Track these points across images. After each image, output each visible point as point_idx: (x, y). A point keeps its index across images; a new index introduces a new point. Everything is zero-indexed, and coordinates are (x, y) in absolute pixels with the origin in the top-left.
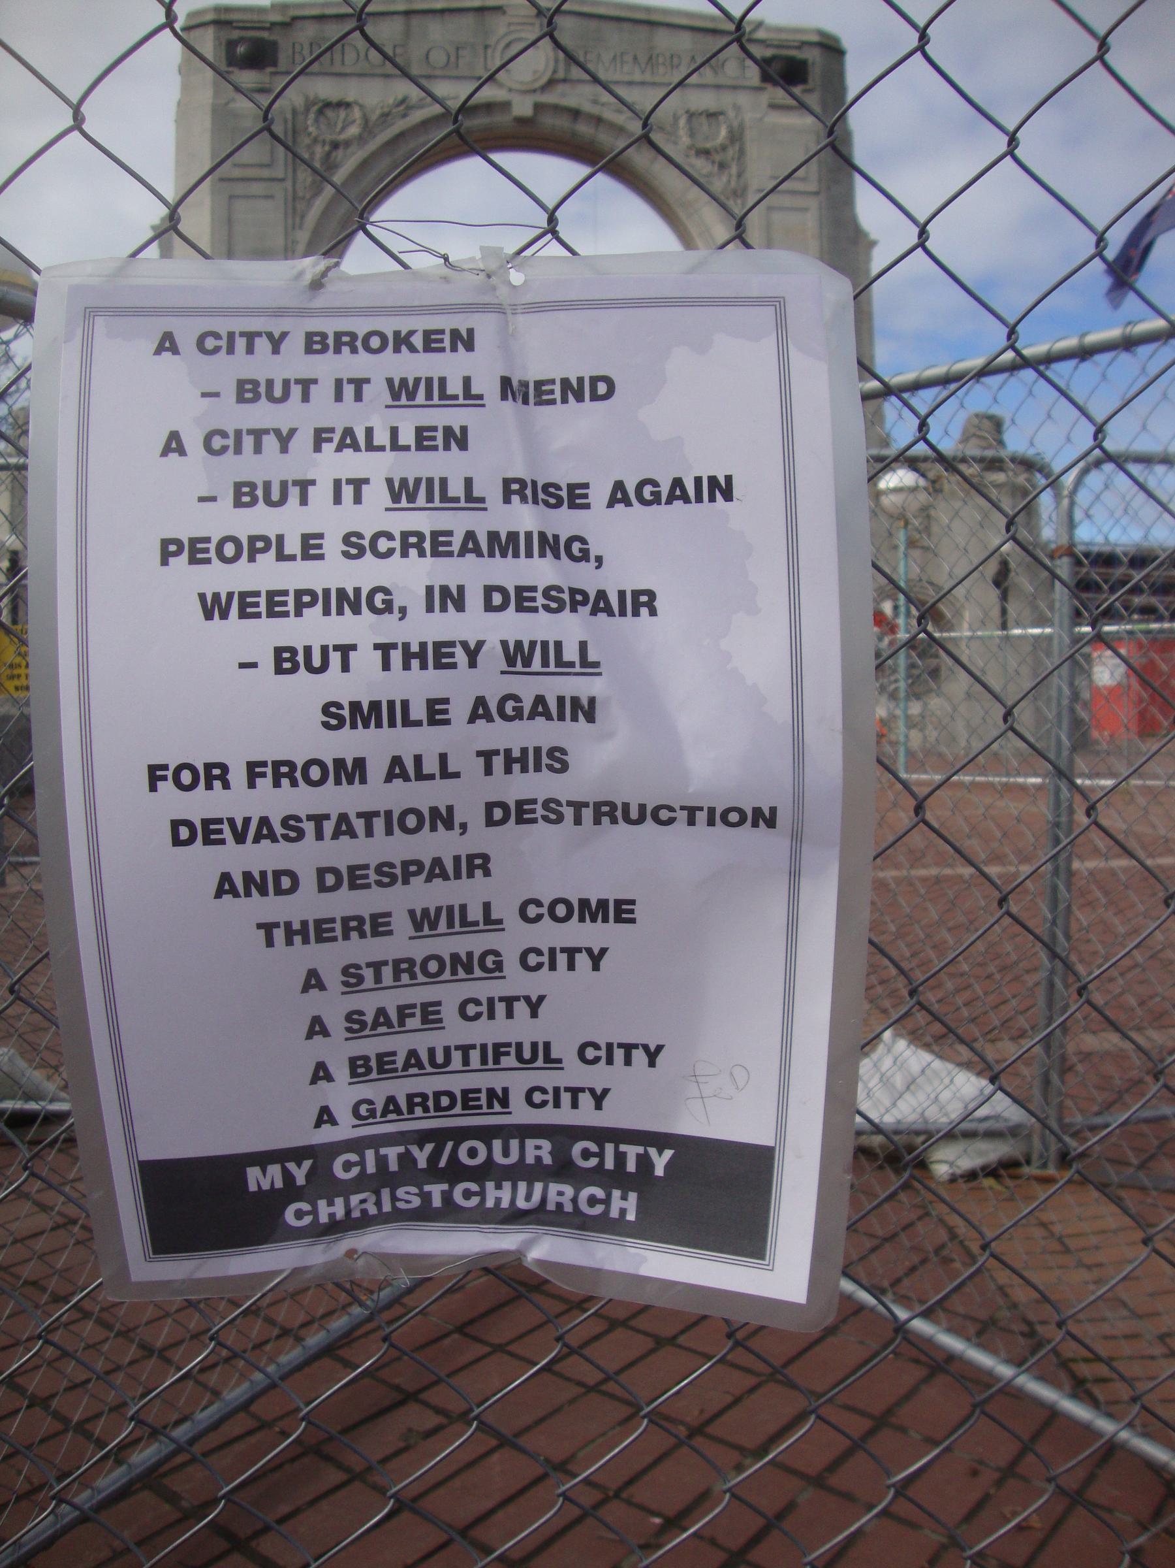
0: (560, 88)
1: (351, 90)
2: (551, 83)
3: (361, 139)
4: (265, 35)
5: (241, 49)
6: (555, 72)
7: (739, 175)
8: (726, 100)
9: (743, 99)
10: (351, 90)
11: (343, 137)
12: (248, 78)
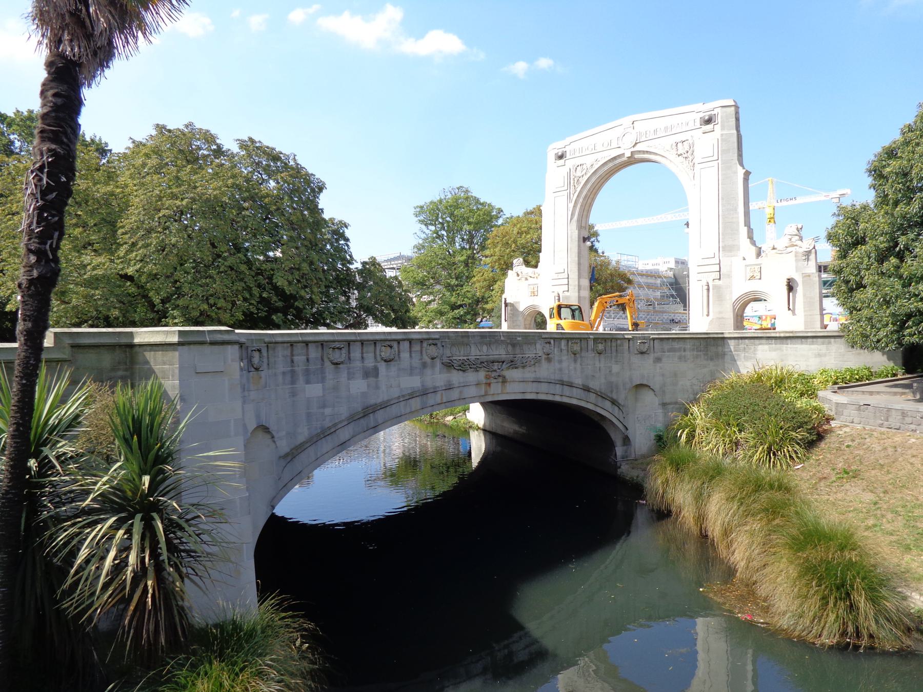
0: (638, 145)
2: (636, 143)
12: (561, 162)
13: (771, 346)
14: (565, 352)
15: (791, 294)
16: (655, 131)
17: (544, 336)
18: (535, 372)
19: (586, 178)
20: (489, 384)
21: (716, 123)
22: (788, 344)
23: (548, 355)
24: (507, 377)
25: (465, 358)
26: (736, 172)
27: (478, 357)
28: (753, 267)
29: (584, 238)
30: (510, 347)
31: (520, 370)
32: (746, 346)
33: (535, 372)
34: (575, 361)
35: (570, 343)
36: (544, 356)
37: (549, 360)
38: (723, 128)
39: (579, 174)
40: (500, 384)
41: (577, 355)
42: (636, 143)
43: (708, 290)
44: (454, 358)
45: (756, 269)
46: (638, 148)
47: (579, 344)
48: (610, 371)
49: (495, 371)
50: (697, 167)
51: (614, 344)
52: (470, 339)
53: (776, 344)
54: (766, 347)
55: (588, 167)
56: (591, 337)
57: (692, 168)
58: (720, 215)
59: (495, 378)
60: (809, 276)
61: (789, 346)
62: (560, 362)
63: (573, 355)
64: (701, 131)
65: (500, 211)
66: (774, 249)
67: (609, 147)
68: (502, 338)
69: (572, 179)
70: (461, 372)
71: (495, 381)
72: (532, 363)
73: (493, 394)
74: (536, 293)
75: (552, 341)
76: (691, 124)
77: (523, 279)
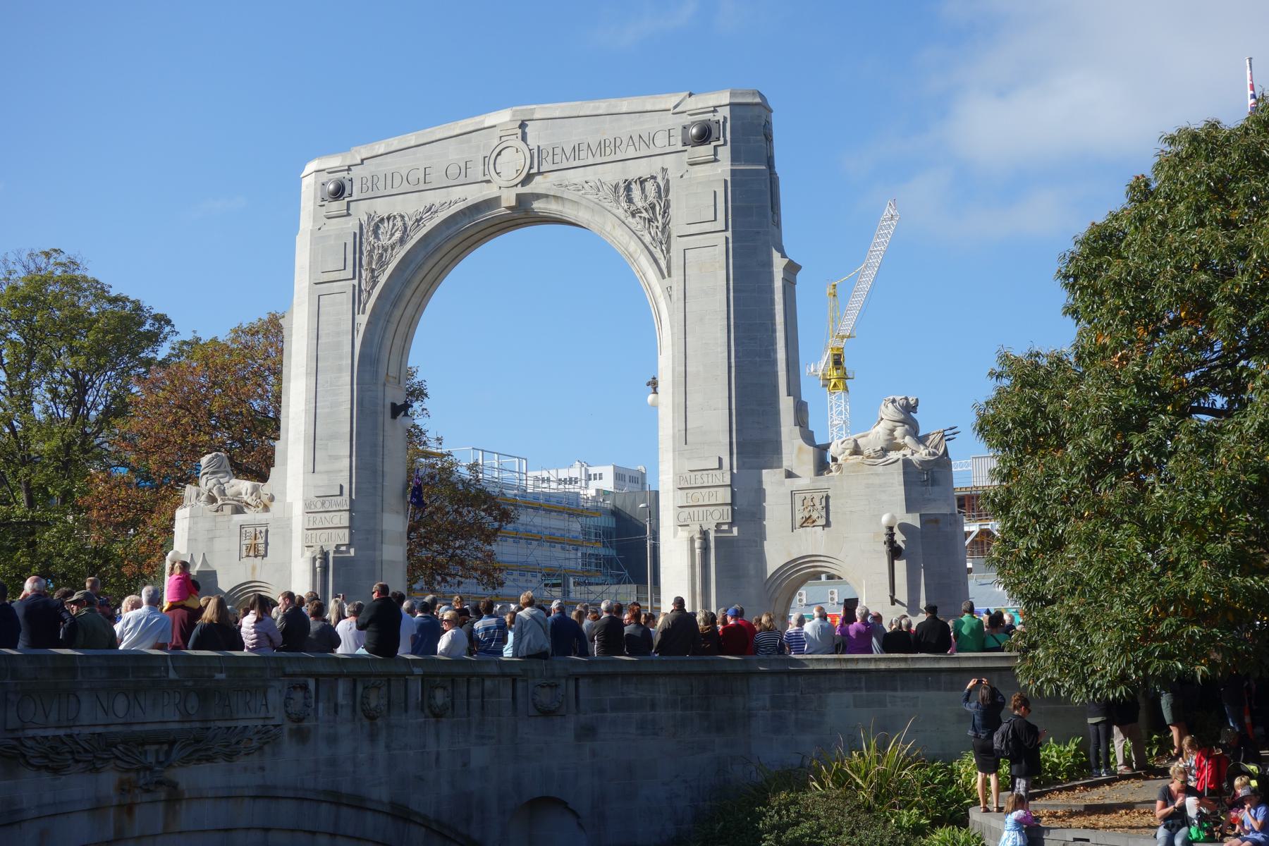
3: (402, 241)
6: (531, 168)
8: (658, 163)
9: (669, 161)
11: (390, 242)
12: (337, 206)
13: (857, 693)
14: (345, 713)
16: (576, 150)
17: (289, 670)
18: (262, 769)
19: (401, 253)
20: (130, 808)
22: (895, 689)
23: (300, 720)
24: (183, 785)
25: (61, 732)
26: (769, 264)
27: (99, 730)
29: (393, 405)
30: (193, 703)
31: (221, 764)
32: (798, 694)
33: (262, 769)
34: (373, 737)
35: (360, 689)
36: (288, 726)
37: (301, 736)
38: (735, 158)
39: (385, 240)
40: (161, 807)
41: (379, 722)
43: (705, 549)
44: (30, 733)
45: (817, 501)
46: (538, 185)
47: (384, 689)
48: (465, 765)
49: (149, 768)
50: (677, 245)
51: (475, 691)
52: (80, 678)
53: (869, 689)
54: (847, 697)
56: (417, 671)
58: (733, 364)
59: (148, 791)
60: (936, 521)
61: (899, 694)
62: (333, 740)
63: (366, 722)
64: (685, 157)
65: (163, 320)
67: (462, 179)
68: (172, 675)
70: (46, 777)
71: (146, 797)
72: (255, 744)
73: (140, 837)
74: (262, 548)
75: (312, 684)
76: (661, 140)
77: (228, 509)
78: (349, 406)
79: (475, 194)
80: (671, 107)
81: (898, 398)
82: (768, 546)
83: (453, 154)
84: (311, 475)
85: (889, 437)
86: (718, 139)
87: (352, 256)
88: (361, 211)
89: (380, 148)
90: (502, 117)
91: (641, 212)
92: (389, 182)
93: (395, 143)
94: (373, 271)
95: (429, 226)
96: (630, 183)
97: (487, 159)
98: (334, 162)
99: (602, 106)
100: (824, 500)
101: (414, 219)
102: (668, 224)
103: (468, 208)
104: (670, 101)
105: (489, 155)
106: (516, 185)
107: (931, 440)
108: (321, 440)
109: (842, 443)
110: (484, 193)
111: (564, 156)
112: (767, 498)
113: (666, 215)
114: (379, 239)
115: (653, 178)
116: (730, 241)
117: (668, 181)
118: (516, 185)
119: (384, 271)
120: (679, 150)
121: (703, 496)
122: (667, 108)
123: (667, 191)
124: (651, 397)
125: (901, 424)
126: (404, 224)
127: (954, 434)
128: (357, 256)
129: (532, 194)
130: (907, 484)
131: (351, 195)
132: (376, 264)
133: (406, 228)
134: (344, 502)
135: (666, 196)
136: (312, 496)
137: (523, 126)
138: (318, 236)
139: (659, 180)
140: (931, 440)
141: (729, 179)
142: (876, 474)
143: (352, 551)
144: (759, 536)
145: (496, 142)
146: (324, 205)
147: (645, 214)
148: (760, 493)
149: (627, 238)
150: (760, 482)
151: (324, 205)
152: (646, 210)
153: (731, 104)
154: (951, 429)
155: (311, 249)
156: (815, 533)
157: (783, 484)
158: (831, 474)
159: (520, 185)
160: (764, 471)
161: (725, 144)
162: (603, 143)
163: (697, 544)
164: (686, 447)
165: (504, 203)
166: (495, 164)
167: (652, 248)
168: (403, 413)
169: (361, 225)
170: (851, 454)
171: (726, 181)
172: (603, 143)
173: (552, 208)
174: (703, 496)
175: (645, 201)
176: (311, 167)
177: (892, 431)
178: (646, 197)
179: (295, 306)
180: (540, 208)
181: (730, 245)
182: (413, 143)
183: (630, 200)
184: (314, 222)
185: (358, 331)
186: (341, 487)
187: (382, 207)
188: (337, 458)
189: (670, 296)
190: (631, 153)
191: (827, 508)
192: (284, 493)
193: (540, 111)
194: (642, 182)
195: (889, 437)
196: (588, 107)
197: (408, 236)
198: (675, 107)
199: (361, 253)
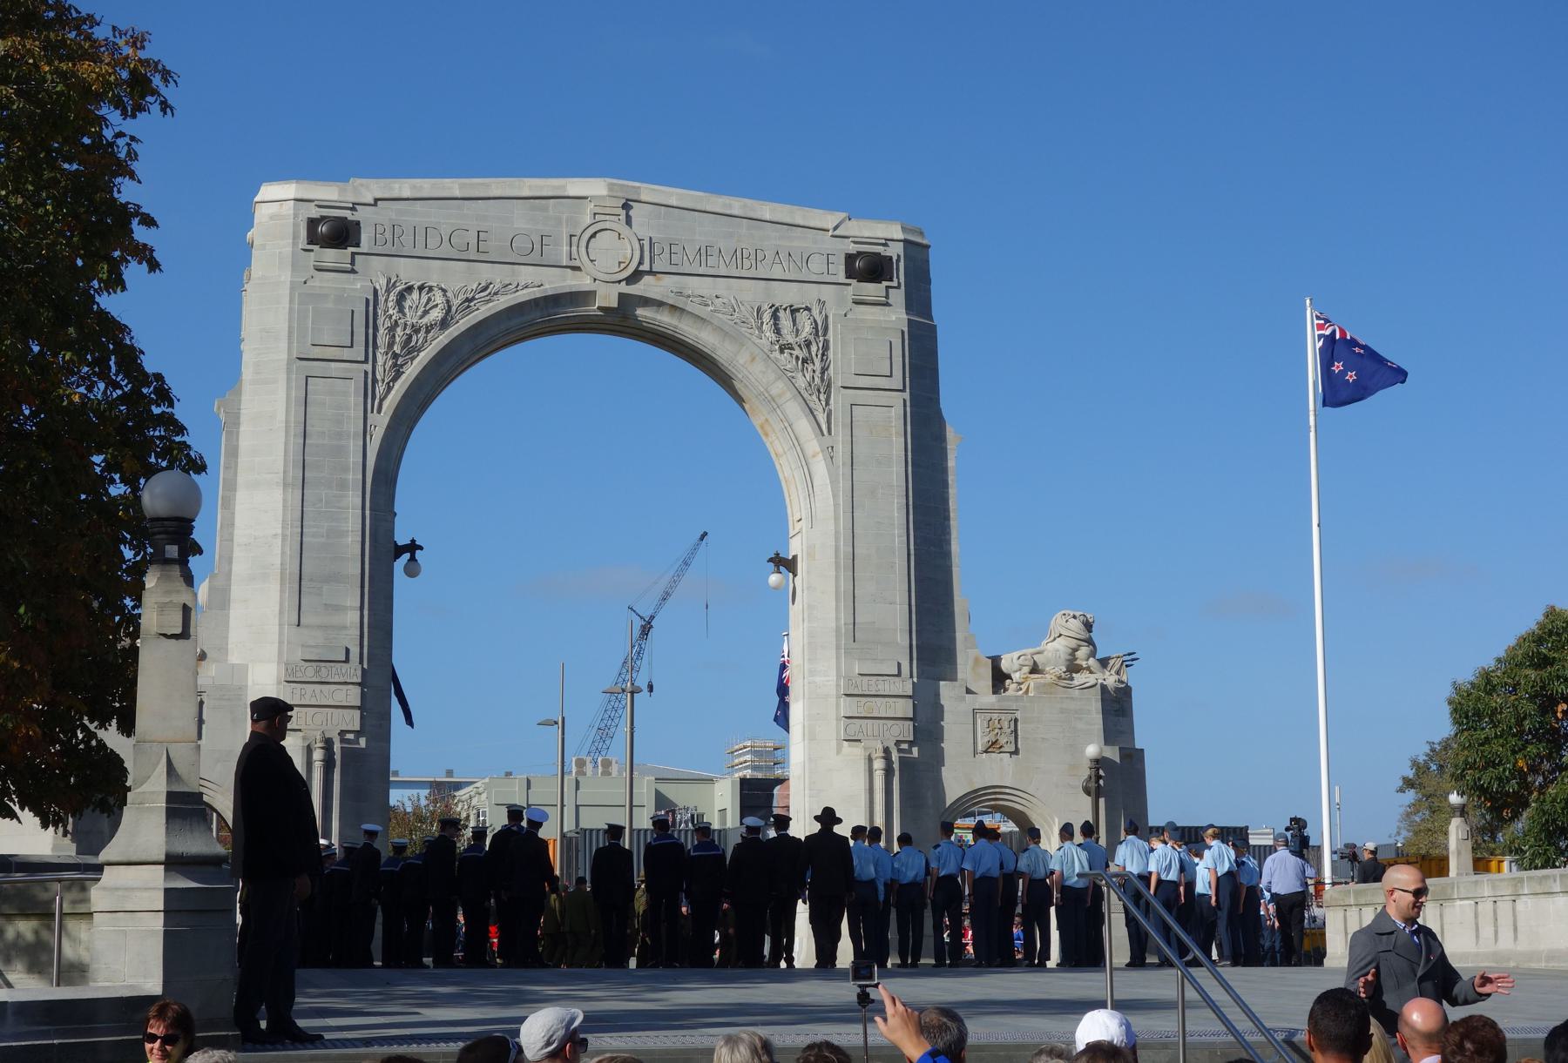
0: (647, 279)
1: (434, 273)
2: (636, 277)
3: (444, 324)
4: (347, 214)
5: (323, 229)
6: (640, 263)
7: (824, 370)
8: (810, 294)
9: (827, 292)
10: (434, 273)
11: (425, 320)
12: (331, 256)
15: (1102, 801)
16: (704, 252)
19: (442, 339)
21: (895, 284)
28: (995, 716)
38: (910, 307)
39: (411, 318)
42: (636, 277)
43: (888, 772)
45: (1006, 725)
50: (839, 400)
55: (456, 303)
57: (823, 397)
58: (912, 552)
66: (1035, 669)
69: (382, 331)
78: (360, 539)
79: (555, 282)
80: (830, 226)
81: (1077, 614)
82: (947, 774)
83: (521, 220)
84: (295, 629)
85: (1070, 657)
86: (891, 280)
87: (364, 329)
88: (376, 273)
89: (404, 188)
90: (595, 187)
91: (792, 349)
92: (420, 239)
93: (427, 186)
94: (395, 356)
95: (483, 312)
96: (777, 310)
97: (575, 240)
98: (327, 192)
99: (737, 205)
100: (1012, 723)
101: (462, 297)
102: (827, 369)
103: (546, 298)
104: (829, 219)
105: (578, 234)
106: (620, 282)
107: (1111, 664)
108: (311, 580)
109: (1019, 658)
110: (569, 282)
111: (685, 258)
112: (946, 715)
113: (825, 358)
114: (404, 315)
115: (807, 309)
116: (908, 404)
117: (826, 317)
118: (620, 282)
119: (413, 359)
120: (840, 282)
121: (881, 707)
122: (825, 227)
123: (826, 329)
124: (774, 579)
125: (1086, 644)
126: (448, 301)
127: (1133, 660)
128: (371, 331)
129: (641, 297)
130: (1105, 712)
131: (358, 245)
132: (403, 348)
133: (450, 307)
134: (353, 672)
135: (825, 335)
136: (299, 654)
137: (626, 206)
138: (303, 296)
139: (815, 312)
140: (1111, 664)
141: (906, 329)
142: (1072, 698)
143: (363, 742)
144: (937, 759)
145: (588, 220)
146: (312, 250)
147: (797, 352)
148: (938, 711)
149: (772, 377)
150: (937, 695)
151: (312, 250)
152: (800, 346)
153: (906, 241)
154: (1130, 654)
155: (291, 309)
156: (1001, 760)
157: (964, 697)
158: (1007, 693)
159: (625, 282)
160: (942, 683)
161: (898, 287)
162: (739, 253)
163: (879, 764)
164: (854, 645)
165: (600, 302)
166: (587, 248)
167: (806, 395)
168: (407, 556)
169: (375, 291)
170: (1031, 673)
171: (903, 332)
172: (739, 253)
173: (664, 319)
174: (881, 707)
175: (797, 336)
176: (268, 191)
177: (1075, 650)
178: (797, 330)
179: (247, 387)
180: (646, 317)
181: (908, 409)
182: (457, 194)
183: (777, 331)
184: (293, 271)
185: (371, 436)
186: (347, 650)
187: (408, 271)
188: (337, 609)
189: (832, 458)
190: (777, 272)
191: (1016, 731)
192: (223, 649)
193: (648, 192)
194: (794, 311)
195: (1070, 657)
196: (718, 203)
197: (452, 319)
198: (835, 228)
199: (376, 328)
